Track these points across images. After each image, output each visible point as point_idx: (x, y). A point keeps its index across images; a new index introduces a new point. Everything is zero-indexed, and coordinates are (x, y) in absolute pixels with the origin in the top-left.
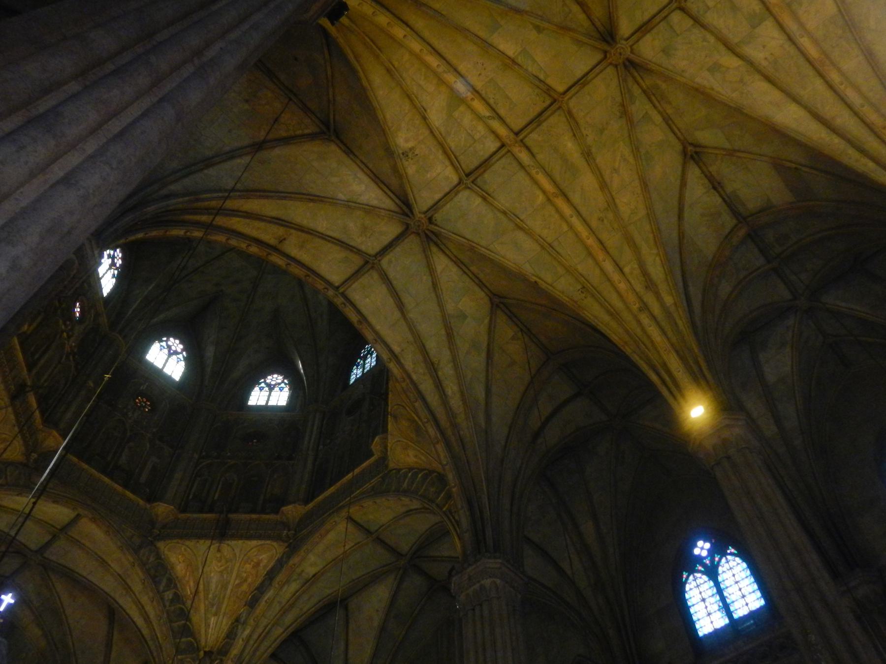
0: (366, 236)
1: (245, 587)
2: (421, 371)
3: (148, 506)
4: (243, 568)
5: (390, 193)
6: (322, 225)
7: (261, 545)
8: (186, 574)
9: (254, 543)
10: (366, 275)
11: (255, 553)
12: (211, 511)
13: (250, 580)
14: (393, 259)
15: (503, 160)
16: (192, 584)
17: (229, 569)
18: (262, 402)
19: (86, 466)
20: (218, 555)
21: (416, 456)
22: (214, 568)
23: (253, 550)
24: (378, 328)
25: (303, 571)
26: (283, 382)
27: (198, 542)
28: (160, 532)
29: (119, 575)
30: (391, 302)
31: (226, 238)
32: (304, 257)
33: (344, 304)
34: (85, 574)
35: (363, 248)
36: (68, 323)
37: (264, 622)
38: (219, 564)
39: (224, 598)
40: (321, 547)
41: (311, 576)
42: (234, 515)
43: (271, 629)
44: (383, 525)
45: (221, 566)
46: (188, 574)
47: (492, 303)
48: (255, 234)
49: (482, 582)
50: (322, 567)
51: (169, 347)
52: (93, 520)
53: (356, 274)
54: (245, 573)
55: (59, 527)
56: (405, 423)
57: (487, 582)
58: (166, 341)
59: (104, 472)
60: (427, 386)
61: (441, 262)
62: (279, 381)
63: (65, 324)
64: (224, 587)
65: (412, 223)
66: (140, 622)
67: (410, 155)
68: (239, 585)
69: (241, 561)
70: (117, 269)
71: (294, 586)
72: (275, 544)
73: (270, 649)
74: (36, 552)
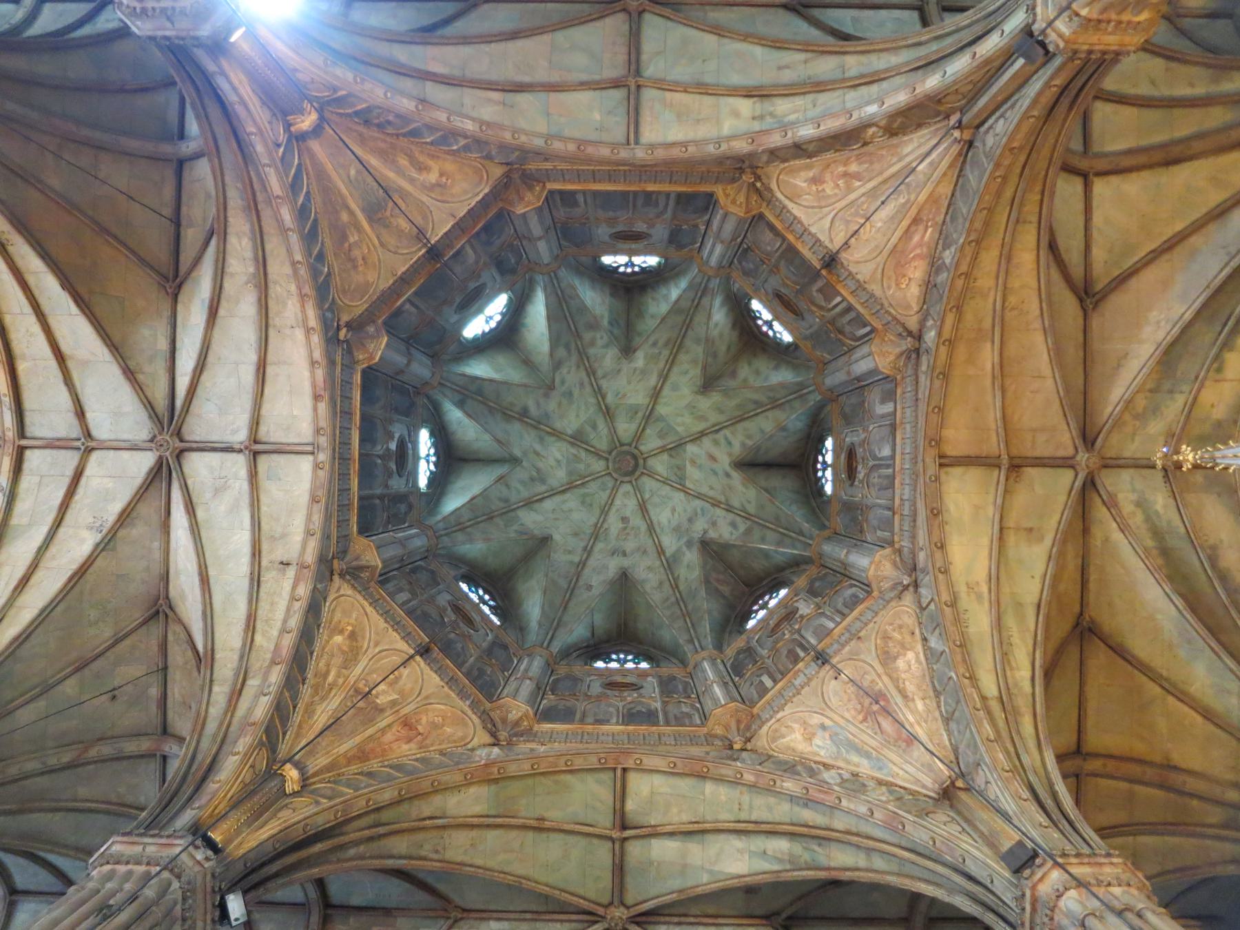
1: (854, 168)
2: (279, 289)
4: (836, 195)
6: (242, 539)
7: (791, 200)
8: (913, 257)
11: (807, 197)
13: (841, 169)
14: (228, 432)
15: (38, 434)
16: (916, 238)
24: (307, 374)
25: (754, 118)
37: (852, 97)
41: (755, 99)
46: (912, 255)
47: (180, 286)
50: (731, 100)
53: (281, 450)
65: (168, 454)
67: (100, 523)
68: (857, 176)
71: (782, 106)
72: (774, 186)
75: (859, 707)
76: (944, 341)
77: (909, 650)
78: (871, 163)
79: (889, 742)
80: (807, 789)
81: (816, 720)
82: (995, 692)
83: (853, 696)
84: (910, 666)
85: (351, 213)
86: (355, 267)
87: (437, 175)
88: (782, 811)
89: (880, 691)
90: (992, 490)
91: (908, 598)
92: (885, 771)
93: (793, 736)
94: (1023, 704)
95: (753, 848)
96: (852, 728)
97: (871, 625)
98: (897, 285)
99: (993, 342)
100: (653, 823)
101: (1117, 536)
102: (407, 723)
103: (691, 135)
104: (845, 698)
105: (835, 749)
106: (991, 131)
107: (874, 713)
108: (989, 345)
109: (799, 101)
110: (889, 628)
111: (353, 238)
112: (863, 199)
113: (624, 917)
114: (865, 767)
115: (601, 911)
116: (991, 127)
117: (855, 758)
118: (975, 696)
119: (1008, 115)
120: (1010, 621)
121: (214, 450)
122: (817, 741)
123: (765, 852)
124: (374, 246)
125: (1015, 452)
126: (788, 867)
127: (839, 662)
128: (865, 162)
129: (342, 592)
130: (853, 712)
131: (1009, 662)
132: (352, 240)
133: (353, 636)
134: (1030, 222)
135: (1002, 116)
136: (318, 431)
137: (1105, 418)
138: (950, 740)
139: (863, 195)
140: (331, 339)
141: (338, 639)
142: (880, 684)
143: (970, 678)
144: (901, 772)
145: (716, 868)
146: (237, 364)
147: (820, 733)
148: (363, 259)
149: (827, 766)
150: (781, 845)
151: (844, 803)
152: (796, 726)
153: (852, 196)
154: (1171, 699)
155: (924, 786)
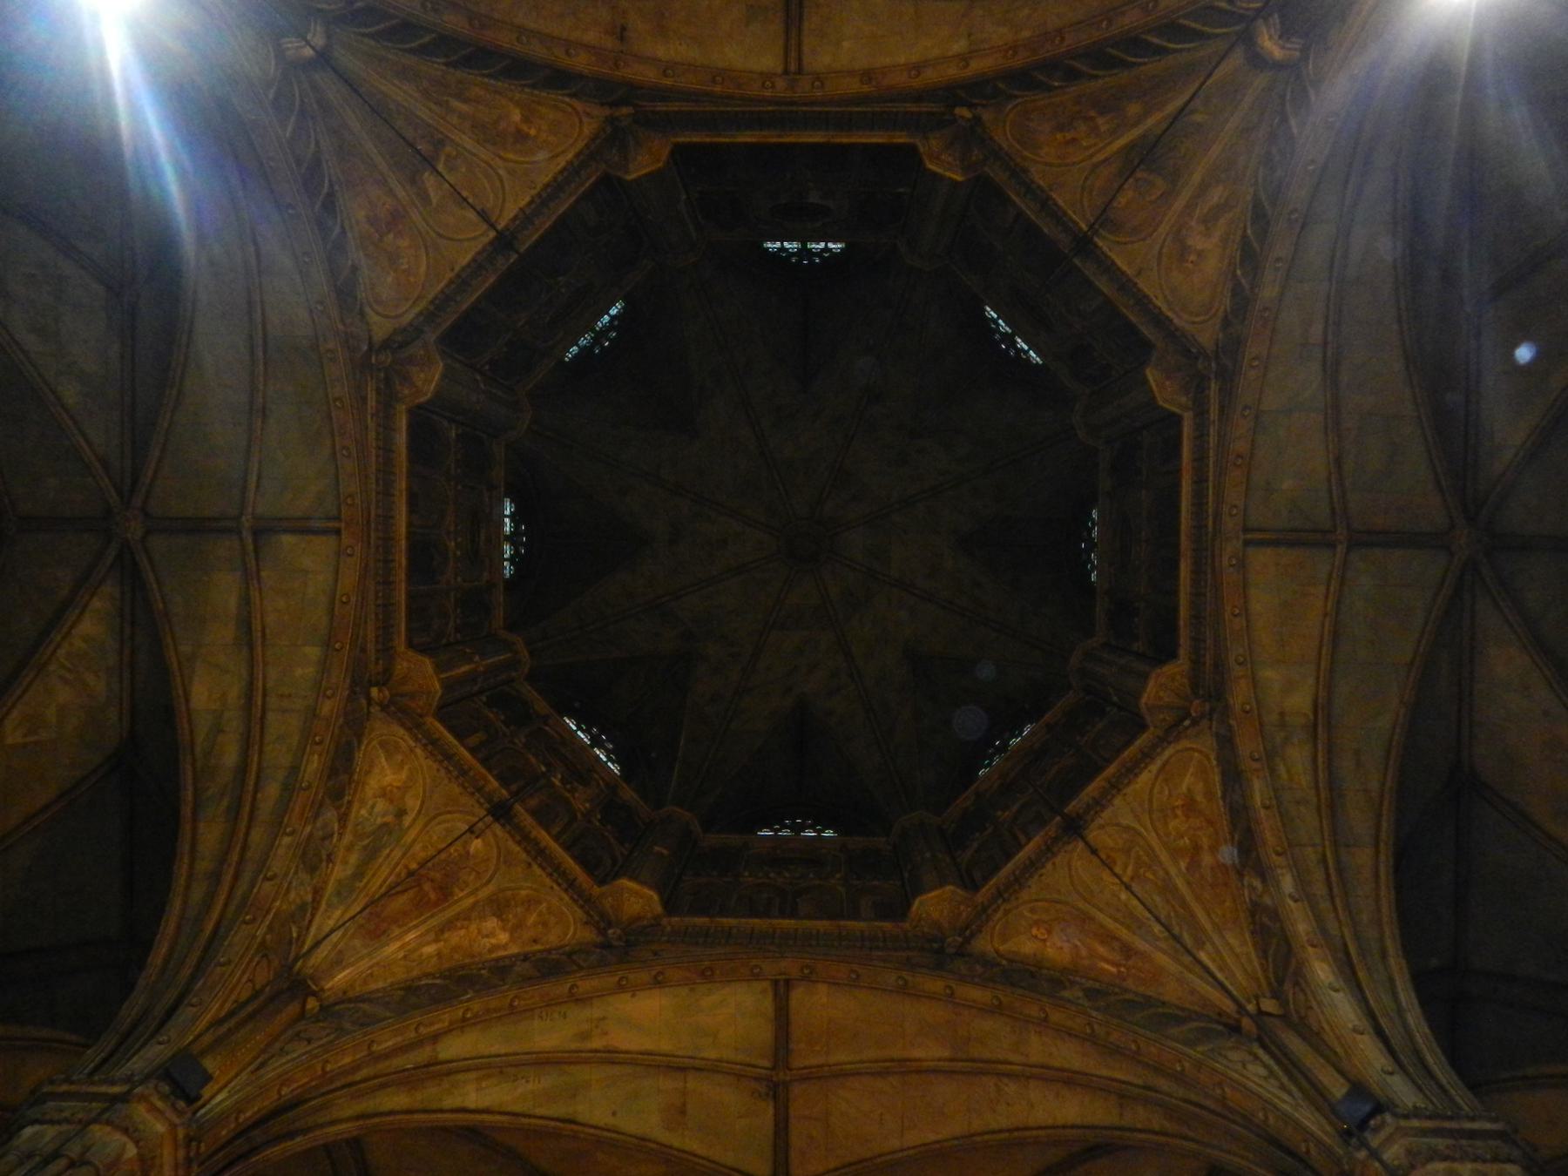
3: (907, 925)
11: (1167, 792)
16: (1101, 950)
17: (1145, 858)
25: (1282, 714)
29: (952, 1060)
34: (895, 1143)
41: (1312, 717)
42: (1074, 803)
44: (1329, 480)
55: (767, 1064)
68: (1194, 864)
72: (1184, 744)
76: (950, 987)
77: (511, 935)
81: (412, 803)
82: (443, 1055)
84: (487, 936)
85: (1139, 121)
86: (1061, 128)
87: (1199, 247)
88: (278, 755)
89: (452, 894)
90: (740, 1057)
91: (589, 935)
92: (335, 900)
93: (388, 772)
94: (429, 1094)
96: (397, 854)
99: (952, 1060)
100: (263, 574)
106: (1251, 1058)
107: (419, 885)
108: (946, 1054)
109: (1305, 780)
111: (1103, 123)
112: (1161, 873)
113: (129, 535)
114: (339, 872)
116: (1256, 1057)
117: (354, 859)
118: (436, 1027)
119: (1272, 1081)
120: (549, 1080)
122: (381, 805)
123: (221, 731)
124: (1091, 156)
125: (796, 1089)
127: (495, 835)
129: (585, 120)
131: (489, 1076)
132: (1100, 121)
133: (521, 137)
134: (1121, 1115)
135: (1271, 1072)
136: (818, 77)
139: (1167, 873)
140: (952, 93)
141: (516, 116)
142: (461, 895)
143: (464, 1019)
148: (1074, 140)
149: (343, 819)
150: (230, 756)
151: (287, 840)
152: (404, 775)
153: (1164, 856)
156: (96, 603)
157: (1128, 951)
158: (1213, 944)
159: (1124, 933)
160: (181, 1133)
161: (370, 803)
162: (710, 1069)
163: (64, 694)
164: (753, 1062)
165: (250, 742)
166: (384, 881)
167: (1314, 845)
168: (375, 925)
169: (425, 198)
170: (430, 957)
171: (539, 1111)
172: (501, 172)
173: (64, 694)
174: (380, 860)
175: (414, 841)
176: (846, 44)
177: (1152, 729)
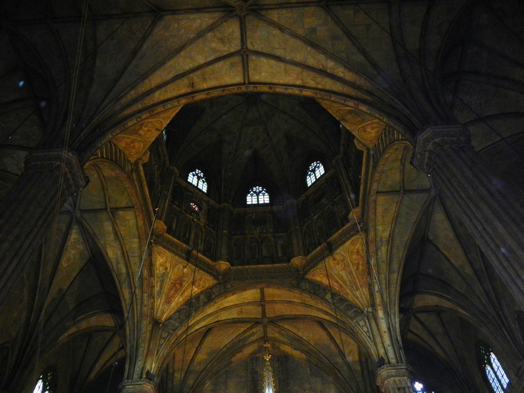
0: (226, 43)
1: (361, 267)
3: (290, 264)
4: (352, 259)
5: (211, 10)
6: (201, 60)
9: (348, 243)
10: (249, 62)
11: (353, 248)
12: (320, 244)
13: (361, 263)
16: (335, 284)
18: (314, 180)
19: (247, 267)
20: (336, 262)
21: (372, 128)
22: (339, 269)
23: (350, 247)
24: (281, 82)
25: (381, 238)
26: (317, 163)
27: (322, 263)
28: (304, 271)
29: (301, 303)
30: (273, 62)
31: (162, 107)
32: (213, 83)
33: (255, 87)
34: (289, 314)
35: (232, 50)
36: (193, 214)
38: (340, 266)
39: (354, 278)
40: (379, 218)
41: (388, 238)
43: (389, 278)
45: (342, 266)
48: (175, 94)
49: (428, 149)
50: (389, 228)
51: (255, 192)
52: (268, 287)
54: (355, 260)
55: (259, 301)
56: (349, 117)
57: (430, 147)
58: (252, 191)
59: (258, 263)
60: (329, 84)
61: (274, 15)
62: (315, 165)
63: (192, 216)
64: (351, 273)
66: (327, 318)
69: (349, 256)
70: (203, 178)
72: (358, 236)
73: (398, 288)
74: (262, 318)
75: (176, 279)
77: (198, 288)
78: (361, 275)
79: (167, 295)
80: (146, 279)
81: (168, 265)
83: (179, 276)
91: (215, 282)
92: (157, 297)
93: (160, 259)
95: (119, 259)
96: (168, 280)
97: (204, 273)
98: (321, 274)
101: (242, 330)
102: (133, 142)
103: (378, 214)
104: (178, 273)
105: (160, 276)
107: (175, 286)
108: (300, 302)
109: (384, 255)
110: (204, 279)
113: (78, 217)
114: (157, 289)
115: (77, 208)
117: (159, 284)
119: (368, 334)
120: (211, 318)
121: (242, 35)
122: (161, 268)
123: (119, 263)
126: (117, 273)
127: (189, 266)
128: (362, 272)
130: (173, 278)
135: (368, 330)
137: (278, 324)
138: (173, 314)
142: (185, 284)
144: (159, 303)
145: (107, 246)
146: (285, 49)
147: (164, 268)
150: (124, 270)
152: (164, 259)
153: (351, 266)
154: (195, 349)
155: (157, 313)
156: (74, 231)
157: (341, 286)
158: (360, 291)
159: (342, 283)
160: (153, 387)
161: (158, 269)
162: (248, 304)
163: (73, 252)
164: (256, 301)
165: (127, 266)
166: (167, 288)
167: (384, 274)
168: (168, 301)
169: (141, 135)
170: (182, 301)
171: (211, 323)
172: (162, 120)
173: (73, 252)
174: (165, 283)
175: (171, 275)
176: (263, 74)
177: (351, 222)
